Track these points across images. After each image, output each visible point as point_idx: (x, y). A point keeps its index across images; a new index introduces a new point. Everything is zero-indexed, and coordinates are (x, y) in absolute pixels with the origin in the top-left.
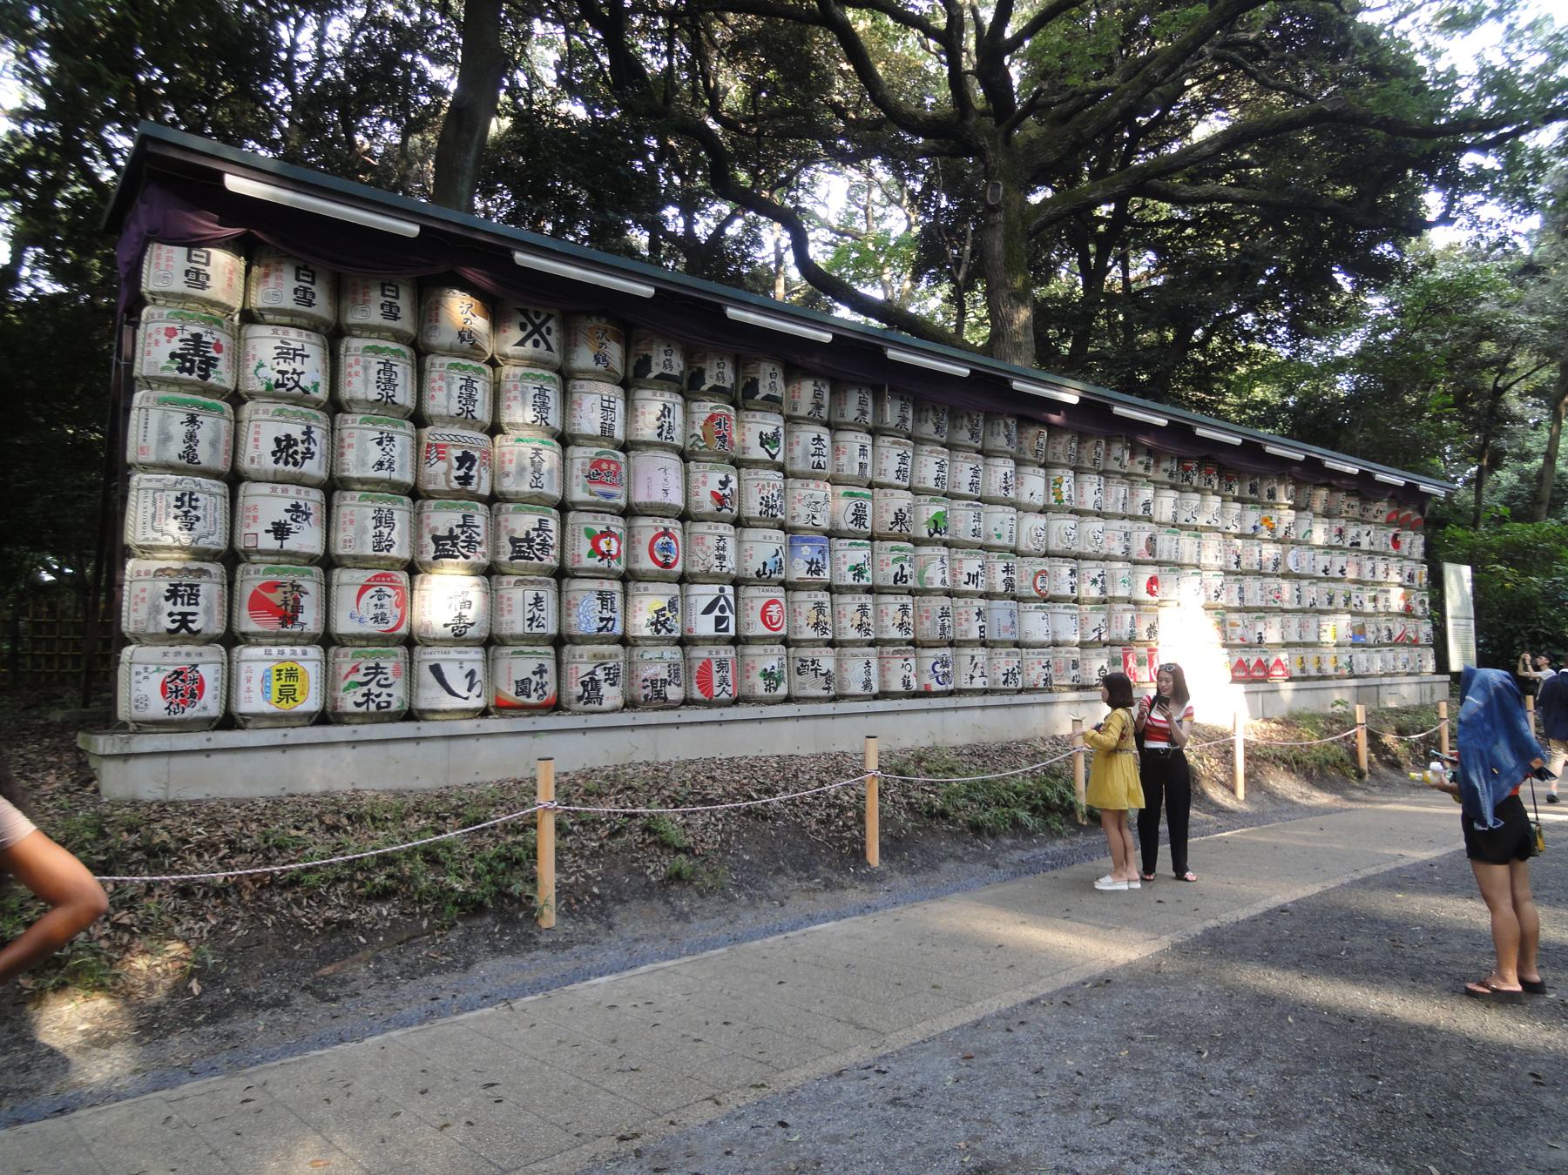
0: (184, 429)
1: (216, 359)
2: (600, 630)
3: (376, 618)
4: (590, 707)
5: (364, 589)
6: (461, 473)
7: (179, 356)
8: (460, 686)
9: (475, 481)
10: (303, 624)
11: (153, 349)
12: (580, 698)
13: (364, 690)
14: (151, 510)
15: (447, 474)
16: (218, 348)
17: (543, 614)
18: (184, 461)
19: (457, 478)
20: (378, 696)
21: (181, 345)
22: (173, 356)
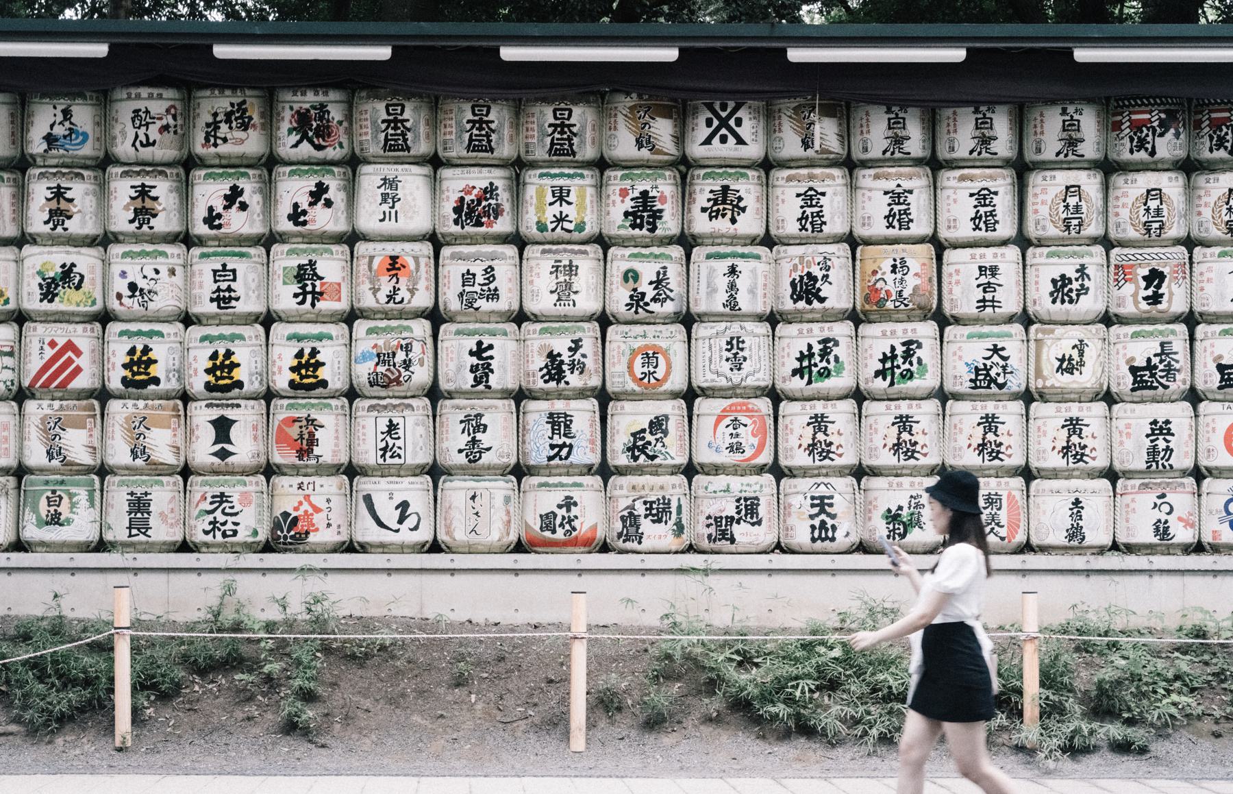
0: (727, 280)
1: (661, 211)
2: (550, 458)
3: (731, 448)
4: (629, 545)
5: (720, 419)
6: (1150, 292)
7: (634, 214)
8: (389, 515)
9: (1165, 298)
10: (318, 457)
11: (611, 209)
12: (620, 535)
13: (211, 518)
14: (708, 354)
15: (1135, 295)
16: (663, 199)
17: (399, 443)
18: (728, 309)
19: (1145, 299)
20: (224, 524)
21: (632, 204)
22: (626, 214)
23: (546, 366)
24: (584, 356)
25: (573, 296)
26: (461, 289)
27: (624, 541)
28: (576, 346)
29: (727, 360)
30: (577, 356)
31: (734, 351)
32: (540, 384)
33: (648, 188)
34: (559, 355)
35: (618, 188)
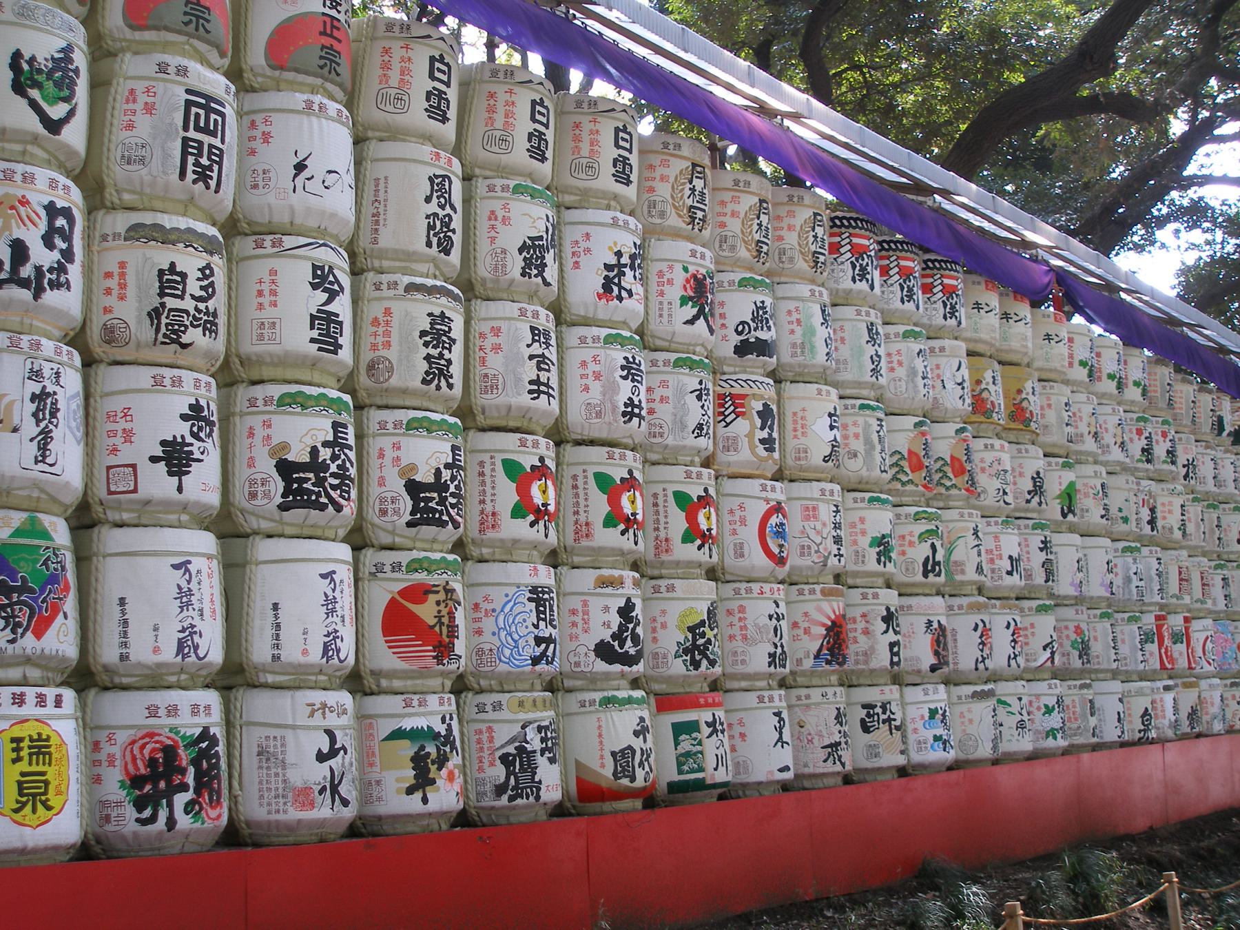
26: (156, 301)
27: (511, 799)
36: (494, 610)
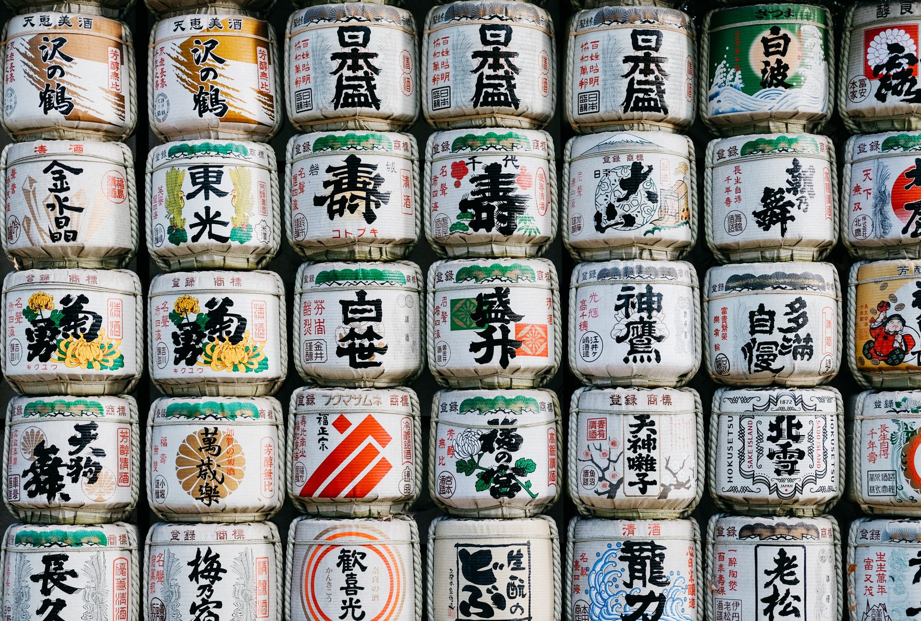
7: (476, 204)
11: (440, 199)
14: (737, 445)
21: (473, 187)
22: (464, 205)
23: (33, 468)
24: (98, 452)
25: (655, 345)
28: (85, 434)
29: (771, 456)
30: (85, 453)
31: (782, 442)
32: (24, 498)
33: (499, 160)
34: (54, 450)
35: (449, 164)
36: (587, 569)
